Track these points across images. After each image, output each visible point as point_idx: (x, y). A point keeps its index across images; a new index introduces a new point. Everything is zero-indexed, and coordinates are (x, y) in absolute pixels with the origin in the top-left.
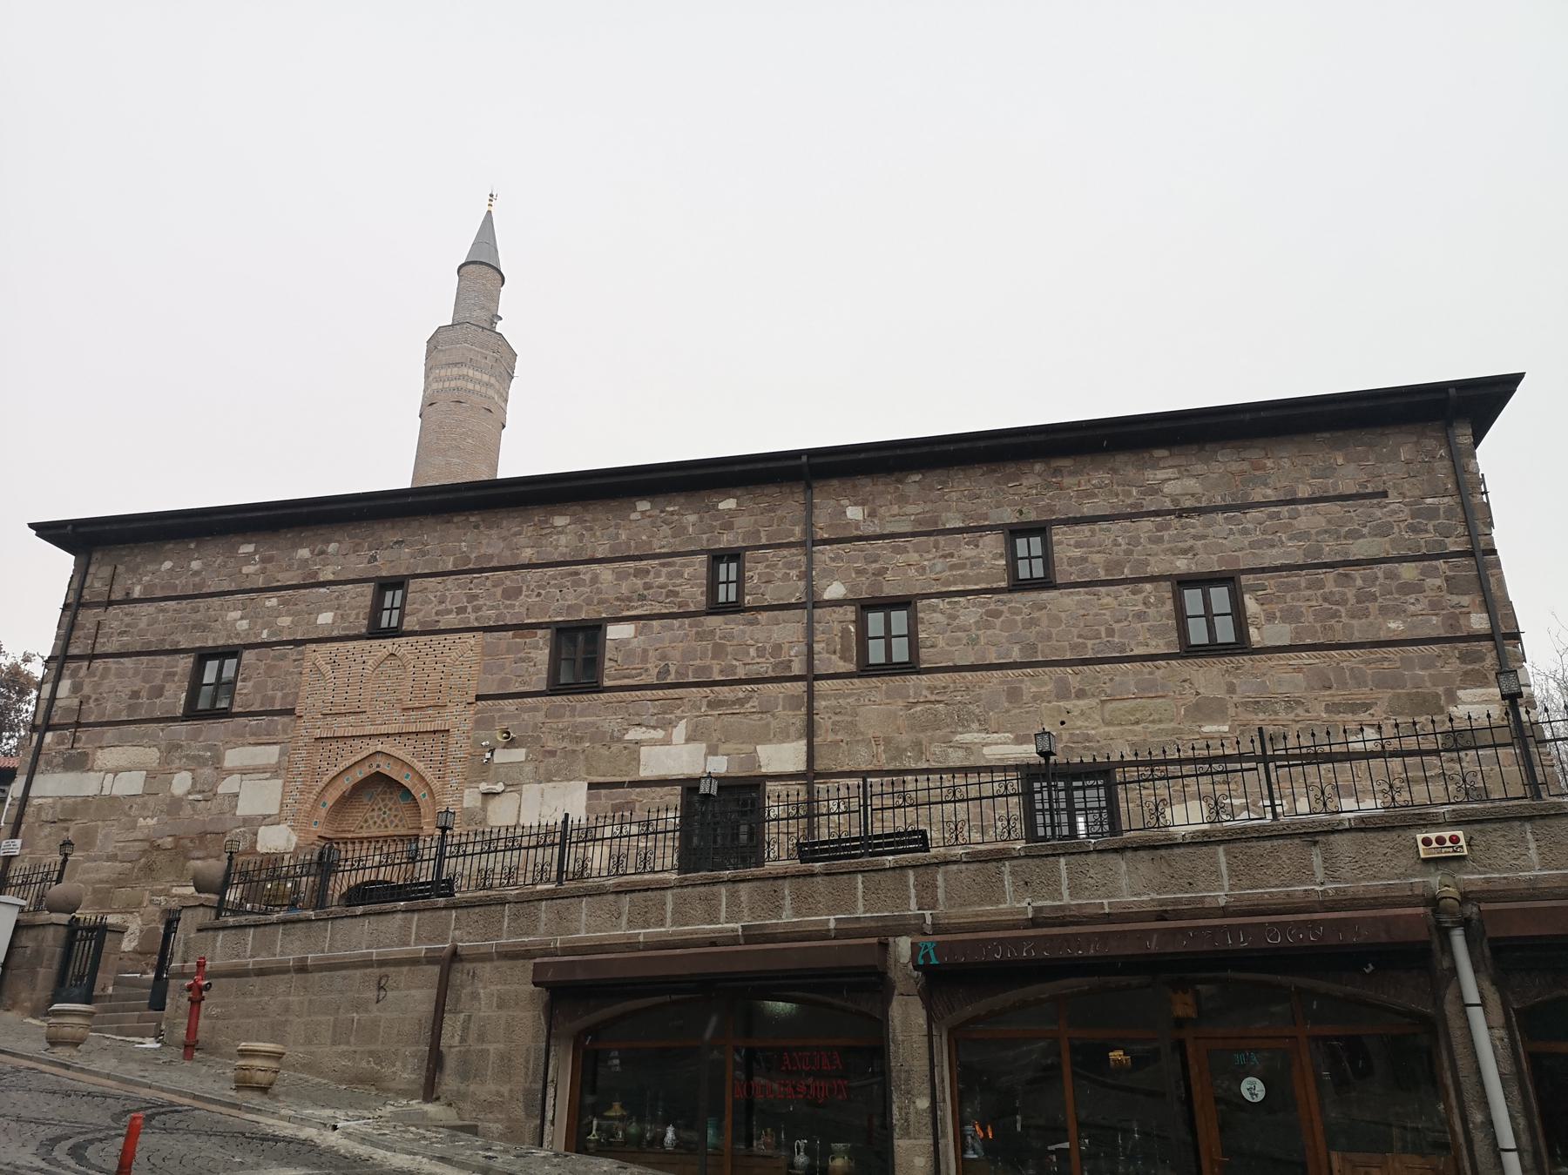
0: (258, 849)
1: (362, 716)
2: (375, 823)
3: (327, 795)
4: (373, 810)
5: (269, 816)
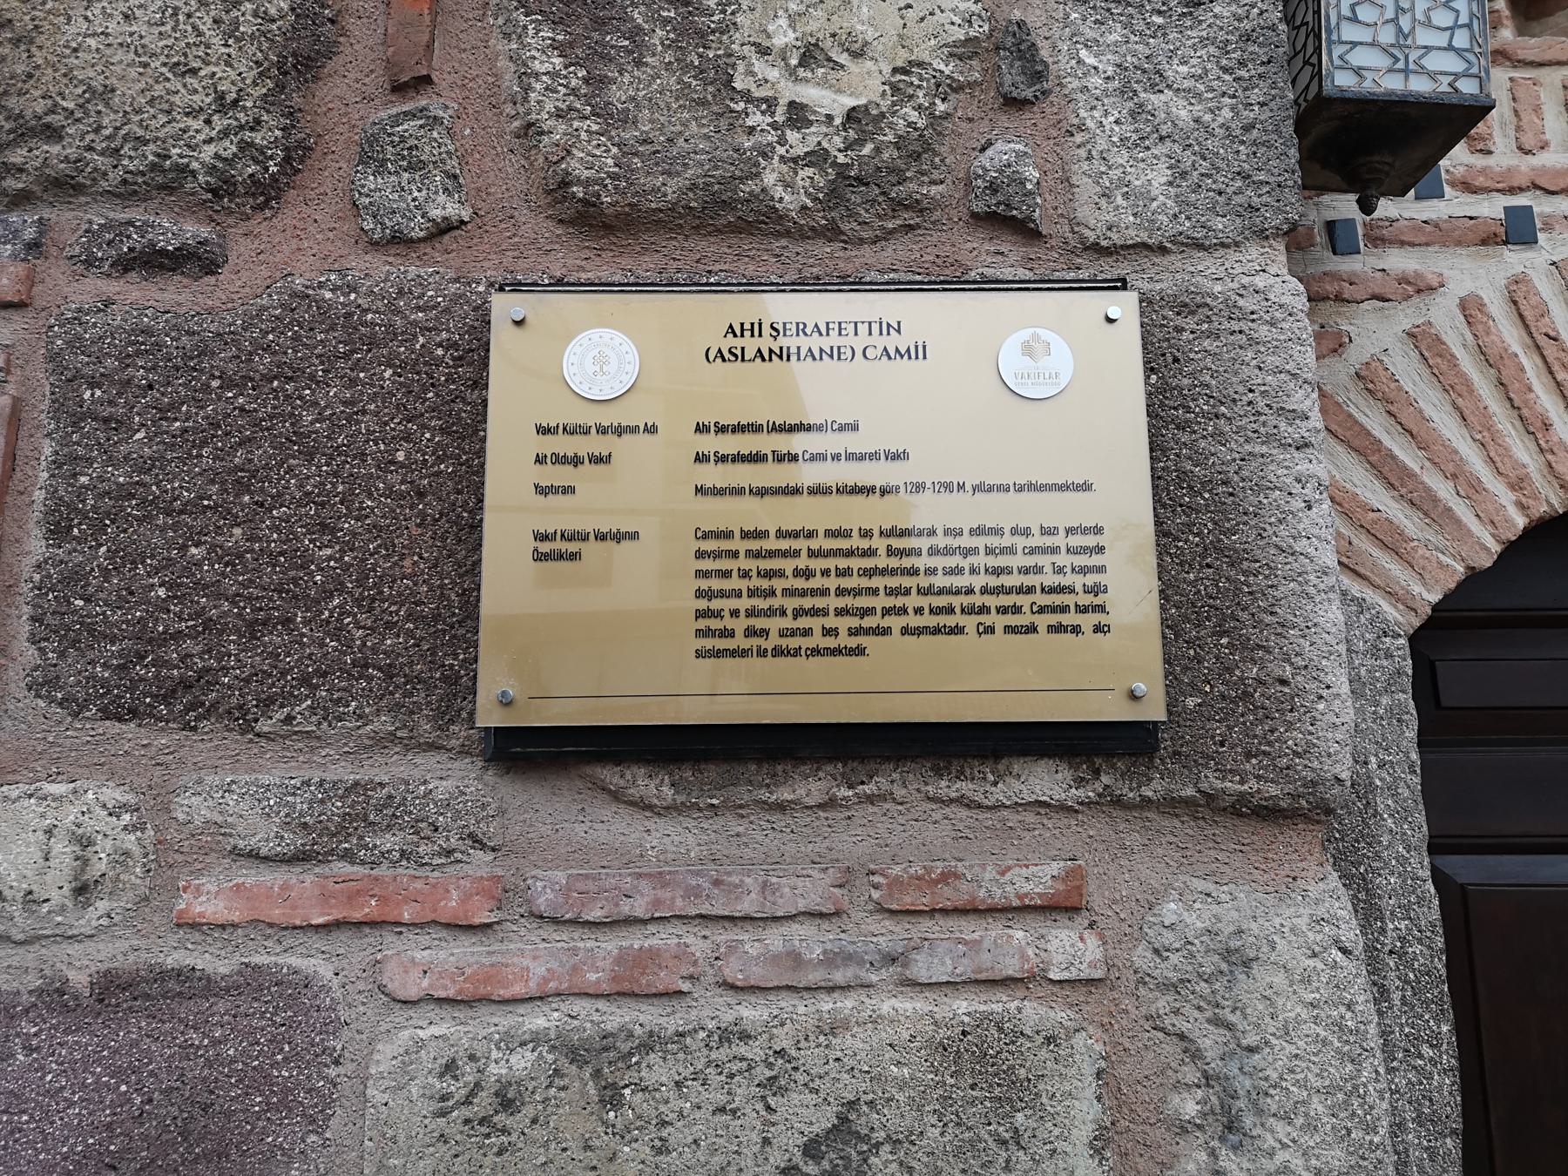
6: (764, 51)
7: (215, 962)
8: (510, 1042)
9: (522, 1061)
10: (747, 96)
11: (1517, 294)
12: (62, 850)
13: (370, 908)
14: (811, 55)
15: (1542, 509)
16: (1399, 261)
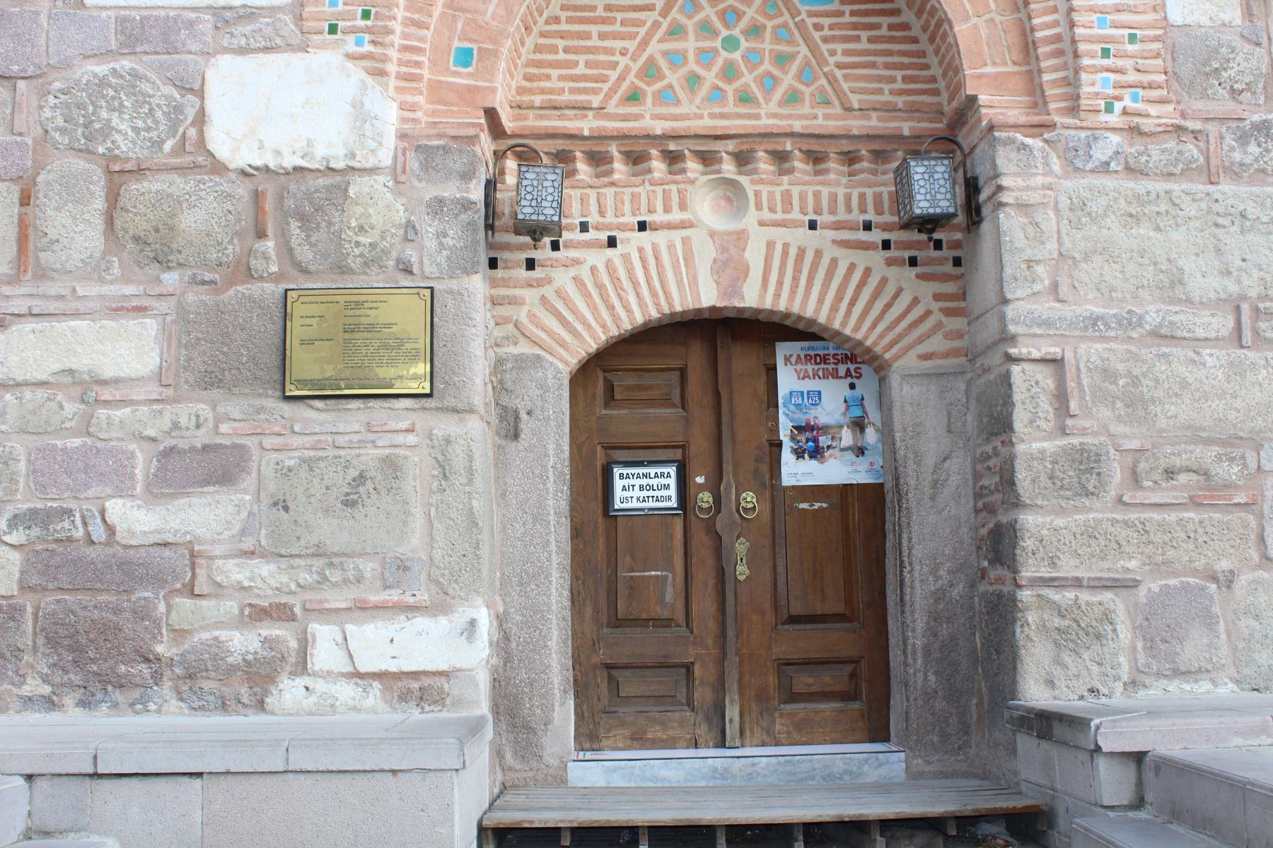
0: (221, 143)
2: (693, 80)
4: (676, 32)
5: (249, 14)
6: (349, 228)
7: (226, 442)
8: (290, 458)
9: (292, 463)
10: (345, 240)
11: (609, 265)
12: (193, 418)
13: (259, 431)
14: (361, 228)
15: (611, 334)
16: (572, 254)
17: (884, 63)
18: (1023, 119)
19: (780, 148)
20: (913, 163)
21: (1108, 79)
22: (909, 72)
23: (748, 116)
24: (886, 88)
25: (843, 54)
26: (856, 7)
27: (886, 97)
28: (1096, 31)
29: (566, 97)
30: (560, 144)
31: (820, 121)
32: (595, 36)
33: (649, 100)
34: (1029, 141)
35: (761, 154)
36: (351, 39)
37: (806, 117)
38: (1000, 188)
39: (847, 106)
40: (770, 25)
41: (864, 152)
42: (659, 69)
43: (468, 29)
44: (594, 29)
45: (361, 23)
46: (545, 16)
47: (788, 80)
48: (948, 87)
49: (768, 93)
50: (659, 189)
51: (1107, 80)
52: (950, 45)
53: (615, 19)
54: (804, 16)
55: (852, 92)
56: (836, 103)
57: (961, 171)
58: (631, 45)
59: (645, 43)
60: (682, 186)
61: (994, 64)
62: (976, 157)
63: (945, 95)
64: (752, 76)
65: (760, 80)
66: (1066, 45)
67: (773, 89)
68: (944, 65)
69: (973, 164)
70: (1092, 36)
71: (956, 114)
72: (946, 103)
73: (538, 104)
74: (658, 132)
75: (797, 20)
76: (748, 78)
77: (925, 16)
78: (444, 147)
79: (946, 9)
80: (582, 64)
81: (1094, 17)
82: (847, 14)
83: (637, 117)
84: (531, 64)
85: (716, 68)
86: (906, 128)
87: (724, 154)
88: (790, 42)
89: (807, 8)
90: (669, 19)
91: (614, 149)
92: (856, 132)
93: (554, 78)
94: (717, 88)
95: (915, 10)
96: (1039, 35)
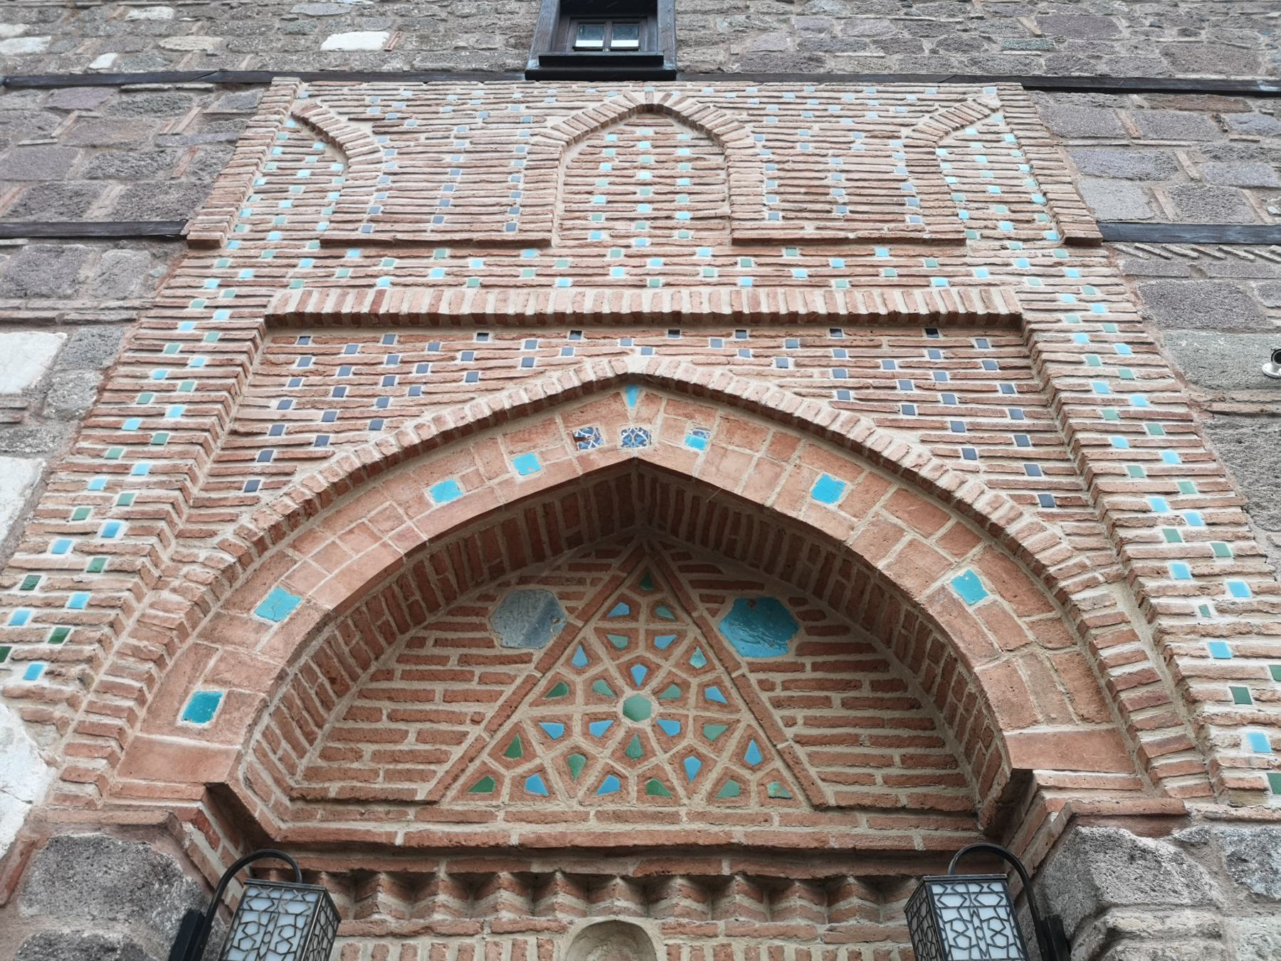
1: (527, 255)
2: (575, 762)
3: (307, 558)
4: (559, 691)
17: (871, 737)
18: (1130, 803)
19: (712, 871)
20: (937, 889)
21: (1262, 737)
22: (911, 751)
23: (656, 817)
24: (879, 775)
25: (805, 724)
26: (820, 659)
27: (879, 789)
28: (1210, 662)
29: (380, 785)
30: (356, 862)
31: (776, 826)
32: (438, 696)
33: (506, 790)
34: (1148, 842)
35: (679, 882)
36: (22, 669)
37: (752, 820)
38: (1114, 935)
39: (816, 801)
40: (694, 682)
41: (851, 880)
42: (527, 743)
43: (222, 666)
44: (439, 688)
45: (45, 647)
46: (373, 669)
47: (723, 761)
48: (977, 773)
49: (691, 784)
50: (506, 942)
51: (1257, 740)
52: (972, 697)
53: (472, 673)
54: (744, 670)
55: (823, 780)
56: (801, 797)
57: (1025, 910)
58: (490, 710)
59: (511, 707)
60: (544, 937)
61: (1051, 721)
62: (1049, 881)
63: (976, 786)
64: (668, 755)
65: (679, 761)
66: (1167, 686)
67: (700, 774)
68: (966, 737)
69: (1045, 897)
70: (1207, 670)
71: (999, 810)
72: (978, 797)
73: (332, 794)
74: (514, 841)
75: (734, 675)
76: (661, 758)
77: (926, 662)
78: (97, 844)
79: (956, 640)
80: (412, 737)
81: (1205, 642)
82: (809, 667)
83: (483, 818)
84: (337, 735)
85: (612, 744)
86: (918, 837)
87: (618, 880)
88: (726, 706)
89: (750, 659)
90: (549, 675)
91: (442, 872)
92: (834, 844)
93: (367, 756)
94: (612, 772)
95: (909, 659)
96: (1116, 672)
